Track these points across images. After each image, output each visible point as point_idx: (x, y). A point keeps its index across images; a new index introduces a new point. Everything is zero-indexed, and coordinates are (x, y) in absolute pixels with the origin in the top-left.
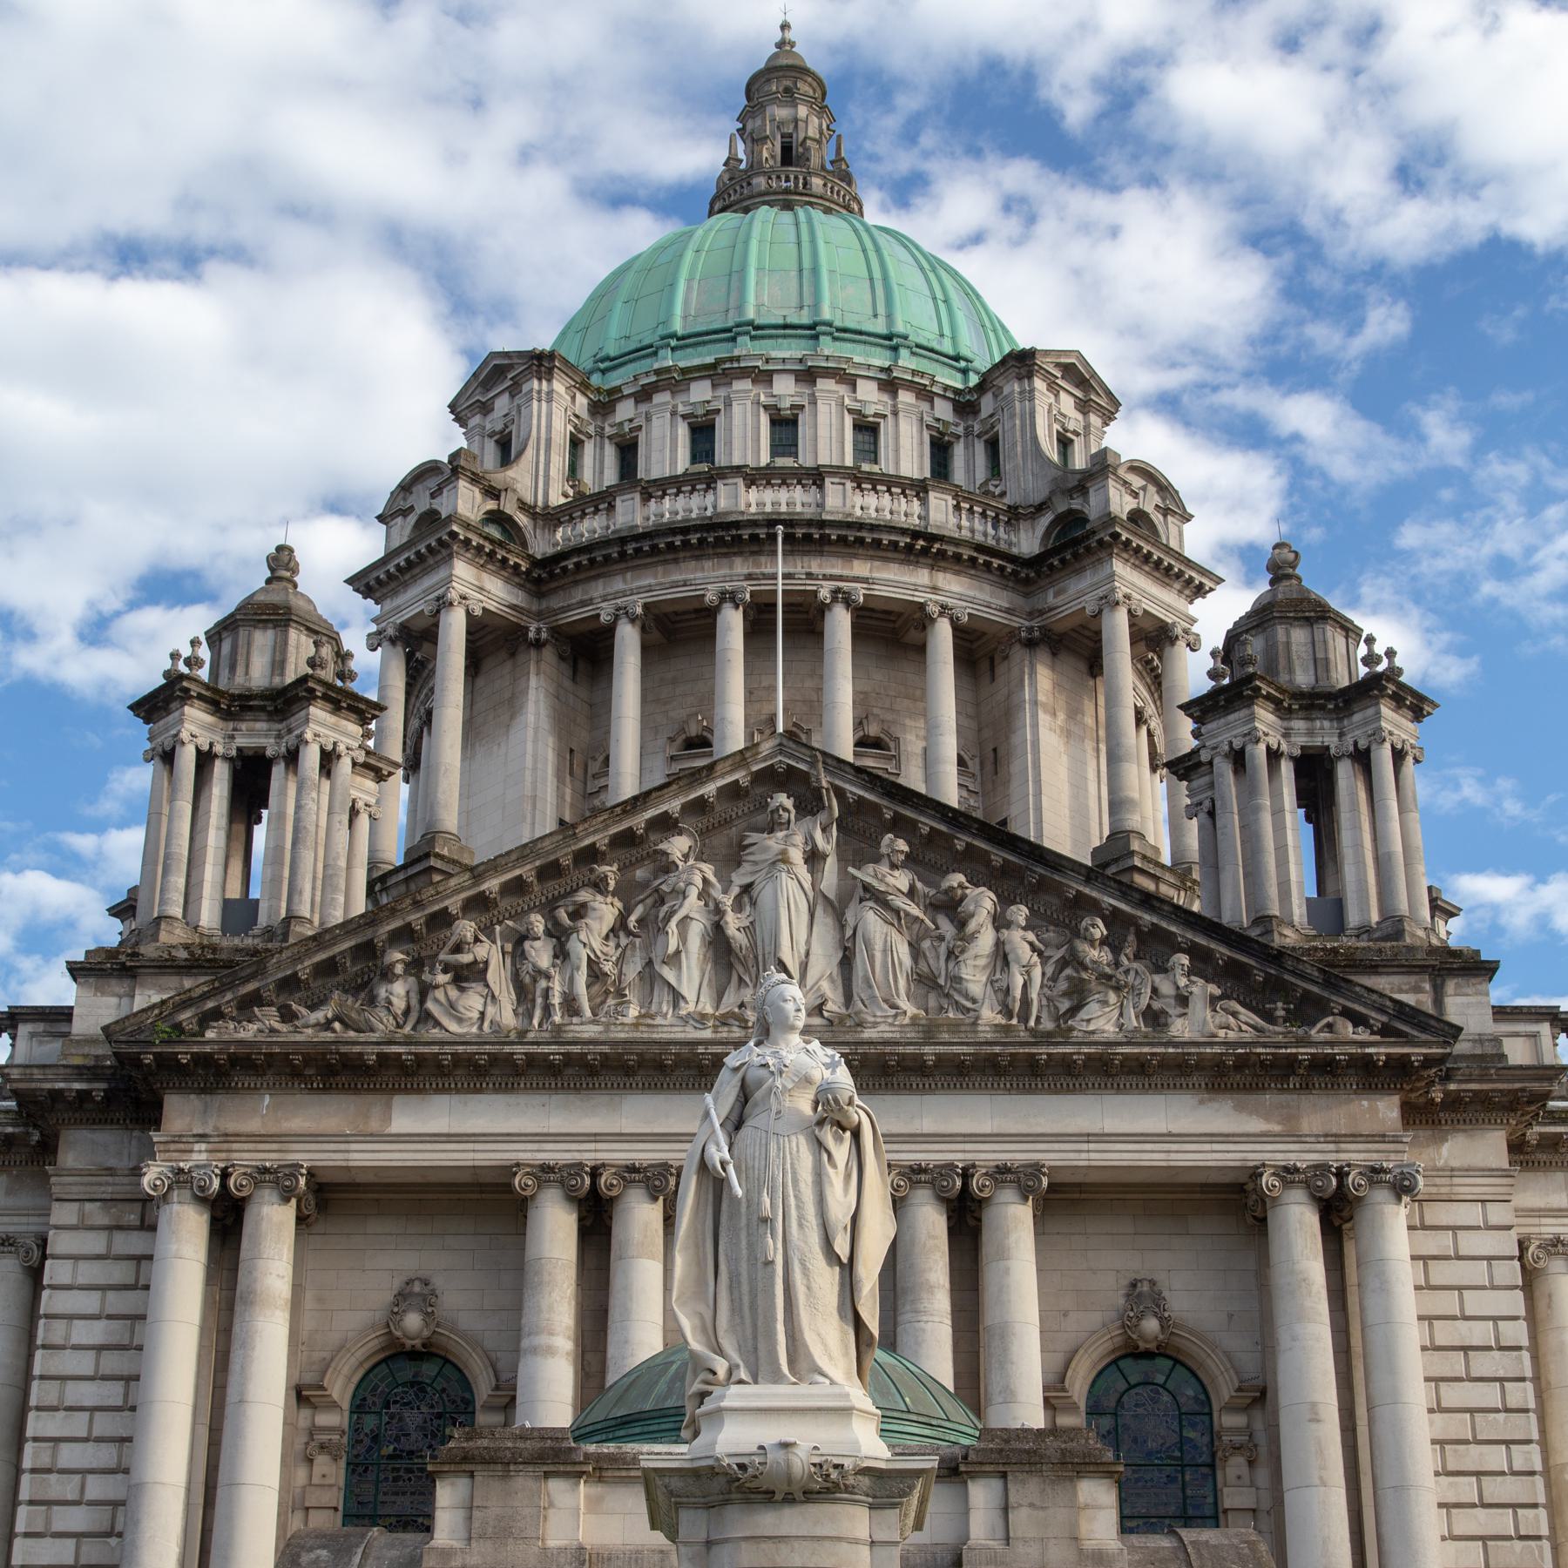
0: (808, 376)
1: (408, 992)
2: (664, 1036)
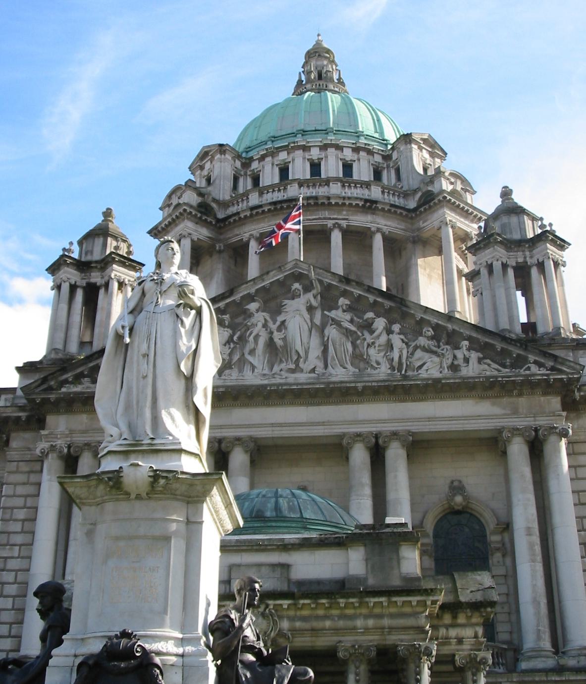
0: (324, 147)
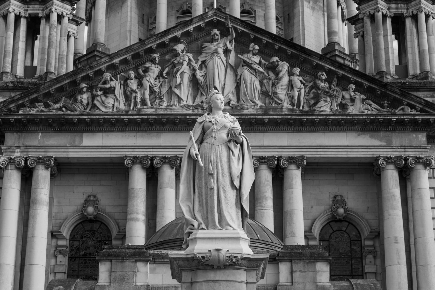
1: (88, 98)
2: (176, 112)
